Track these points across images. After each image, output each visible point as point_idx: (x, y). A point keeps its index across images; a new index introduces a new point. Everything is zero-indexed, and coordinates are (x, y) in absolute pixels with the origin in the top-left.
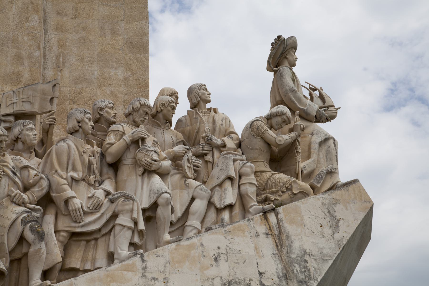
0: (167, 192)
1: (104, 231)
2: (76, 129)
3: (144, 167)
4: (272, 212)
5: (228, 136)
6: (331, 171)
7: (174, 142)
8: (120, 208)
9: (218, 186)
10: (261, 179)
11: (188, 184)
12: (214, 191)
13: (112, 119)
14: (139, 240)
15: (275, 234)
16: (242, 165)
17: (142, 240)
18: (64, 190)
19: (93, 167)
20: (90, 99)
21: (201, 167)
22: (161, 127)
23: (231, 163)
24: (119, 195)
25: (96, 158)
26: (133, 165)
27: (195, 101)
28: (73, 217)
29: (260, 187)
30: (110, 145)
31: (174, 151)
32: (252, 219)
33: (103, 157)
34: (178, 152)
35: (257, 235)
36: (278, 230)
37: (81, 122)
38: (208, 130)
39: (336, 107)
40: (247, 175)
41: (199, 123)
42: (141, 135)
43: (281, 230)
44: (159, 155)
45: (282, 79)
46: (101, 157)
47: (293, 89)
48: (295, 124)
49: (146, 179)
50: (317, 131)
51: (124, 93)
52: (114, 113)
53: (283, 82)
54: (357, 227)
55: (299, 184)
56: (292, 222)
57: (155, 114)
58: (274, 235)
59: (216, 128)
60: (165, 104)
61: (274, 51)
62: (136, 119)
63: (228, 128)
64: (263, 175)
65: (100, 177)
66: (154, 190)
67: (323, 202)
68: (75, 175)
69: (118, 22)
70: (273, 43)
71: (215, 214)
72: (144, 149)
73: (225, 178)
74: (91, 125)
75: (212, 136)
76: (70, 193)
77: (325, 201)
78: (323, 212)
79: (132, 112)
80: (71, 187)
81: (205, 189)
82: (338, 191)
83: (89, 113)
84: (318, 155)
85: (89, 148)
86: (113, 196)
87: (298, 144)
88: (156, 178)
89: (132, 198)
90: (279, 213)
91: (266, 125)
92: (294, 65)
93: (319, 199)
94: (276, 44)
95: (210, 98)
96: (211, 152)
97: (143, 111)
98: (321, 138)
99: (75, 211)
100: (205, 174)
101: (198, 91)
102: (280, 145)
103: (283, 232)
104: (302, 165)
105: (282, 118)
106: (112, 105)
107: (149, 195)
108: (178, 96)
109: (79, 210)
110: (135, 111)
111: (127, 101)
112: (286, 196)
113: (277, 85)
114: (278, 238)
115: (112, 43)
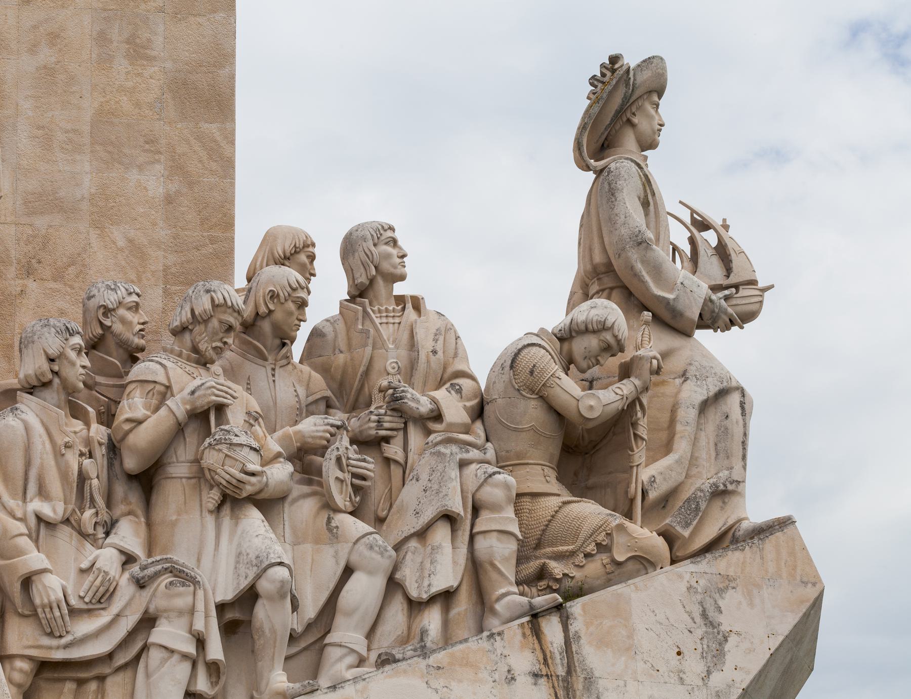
0: (281, 564)
1: (121, 660)
2: (45, 380)
3: (221, 489)
4: (553, 614)
5: (448, 385)
6: (724, 488)
7: (302, 402)
8: (160, 603)
9: (415, 538)
10: (531, 517)
11: (335, 531)
12: (405, 550)
13: (137, 341)
14: (209, 684)
15: (558, 676)
16: (482, 480)
17: (216, 685)
18: (20, 552)
19: (90, 486)
20: (73, 263)
21: (371, 478)
22: (266, 359)
23: (454, 473)
24: (159, 567)
25: (96, 460)
26: (193, 481)
27: (362, 279)
28: (44, 622)
29: (527, 538)
30: (133, 425)
31: (300, 431)
32: (499, 634)
33: (115, 454)
34: (313, 437)
35: (509, 676)
36: (566, 665)
37: (57, 360)
38: (396, 369)
39: (761, 285)
40: (495, 508)
41: (369, 349)
42: (214, 398)
43: (574, 664)
44: (261, 456)
45: (612, 202)
46: (108, 453)
47: (640, 237)
48: (639, 352)
49: (227, 522)
50: (699, 367)
51: (163, 247)
52: (142, 321)
53: (616, 211)
54: (771, 654)
55: (630, 535)
56: (602, 642)
57: (250, 320)
58: (554, 678)
59: (418, 362)
60: (278, 295)
61: (596, 109)
62: (199, 345)
63: (451, 360)
64: (535, 513)
65: (108, 510)
66: (248, 554)
67: (692, 584)
68: (47, 510)
69: (148, 18)
70: (595, 76)
71: (404, 614)
72: (223, 441)
73: (435, 516)
74: (84, 367)
75: (405, 387)
76: (34, 559)
77: (697, 582)
78: (687, 612)
79: (192, 323)
80: (36, 541)
81: (380, 547)
82: (735, 552)
83: (78, 333)
84: (695, 442)
85: (77, 429)
86: (144, 569)
87: (639, 414)
88: (254, 517)
89: (191, 577)
90: (571, 616)
91: (555, 357)
92: (653, 145)
93: (680, 577)
94: (603, 83)
95: (405, 266)
96: (401, 433)
97: (221, 322)
98: (708, 389)
99: (48, 607)
100: (384, 496)
101: (373, 248)
102: (591, 419)
103: (577, 668)
104: (645, 474)
105: (602, 338)
106: (134, 298)
107: (236, 568)
108: (313, 253)
109: (60, 606)
110: (199, 323)
111: (173, 270)
112: (594, 568)
113: (599, 216)
114: (564, 687)
115: (130, 84)
